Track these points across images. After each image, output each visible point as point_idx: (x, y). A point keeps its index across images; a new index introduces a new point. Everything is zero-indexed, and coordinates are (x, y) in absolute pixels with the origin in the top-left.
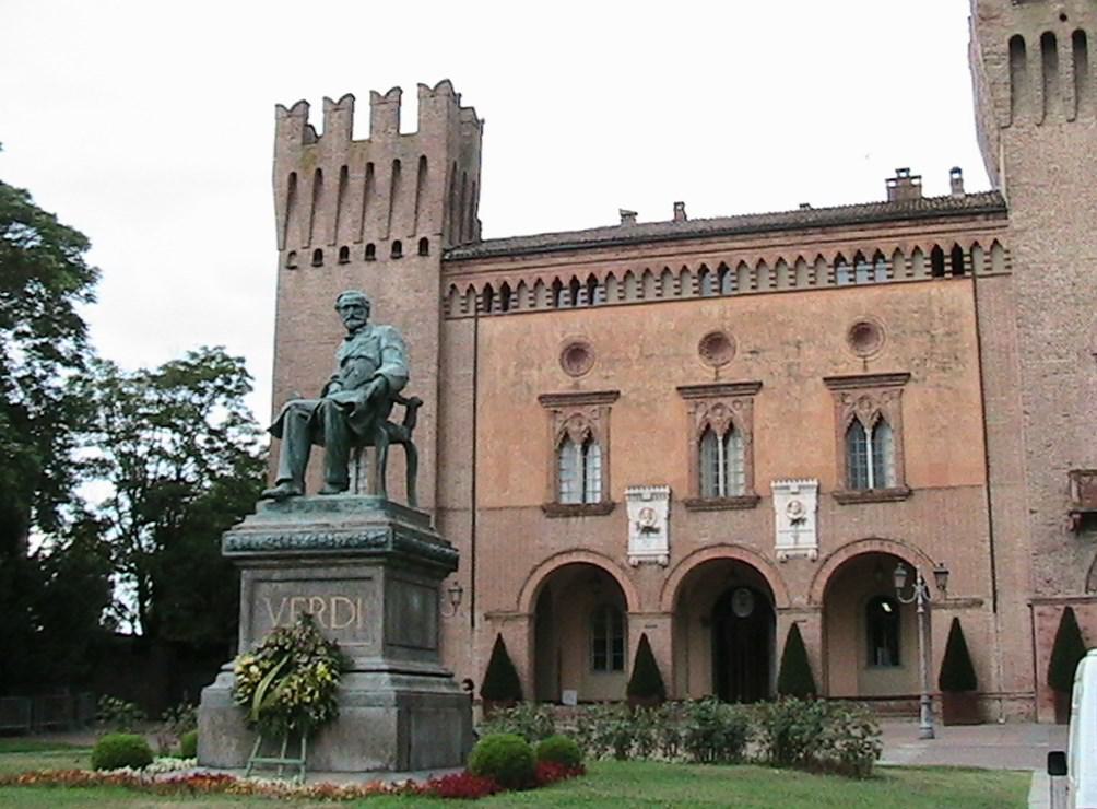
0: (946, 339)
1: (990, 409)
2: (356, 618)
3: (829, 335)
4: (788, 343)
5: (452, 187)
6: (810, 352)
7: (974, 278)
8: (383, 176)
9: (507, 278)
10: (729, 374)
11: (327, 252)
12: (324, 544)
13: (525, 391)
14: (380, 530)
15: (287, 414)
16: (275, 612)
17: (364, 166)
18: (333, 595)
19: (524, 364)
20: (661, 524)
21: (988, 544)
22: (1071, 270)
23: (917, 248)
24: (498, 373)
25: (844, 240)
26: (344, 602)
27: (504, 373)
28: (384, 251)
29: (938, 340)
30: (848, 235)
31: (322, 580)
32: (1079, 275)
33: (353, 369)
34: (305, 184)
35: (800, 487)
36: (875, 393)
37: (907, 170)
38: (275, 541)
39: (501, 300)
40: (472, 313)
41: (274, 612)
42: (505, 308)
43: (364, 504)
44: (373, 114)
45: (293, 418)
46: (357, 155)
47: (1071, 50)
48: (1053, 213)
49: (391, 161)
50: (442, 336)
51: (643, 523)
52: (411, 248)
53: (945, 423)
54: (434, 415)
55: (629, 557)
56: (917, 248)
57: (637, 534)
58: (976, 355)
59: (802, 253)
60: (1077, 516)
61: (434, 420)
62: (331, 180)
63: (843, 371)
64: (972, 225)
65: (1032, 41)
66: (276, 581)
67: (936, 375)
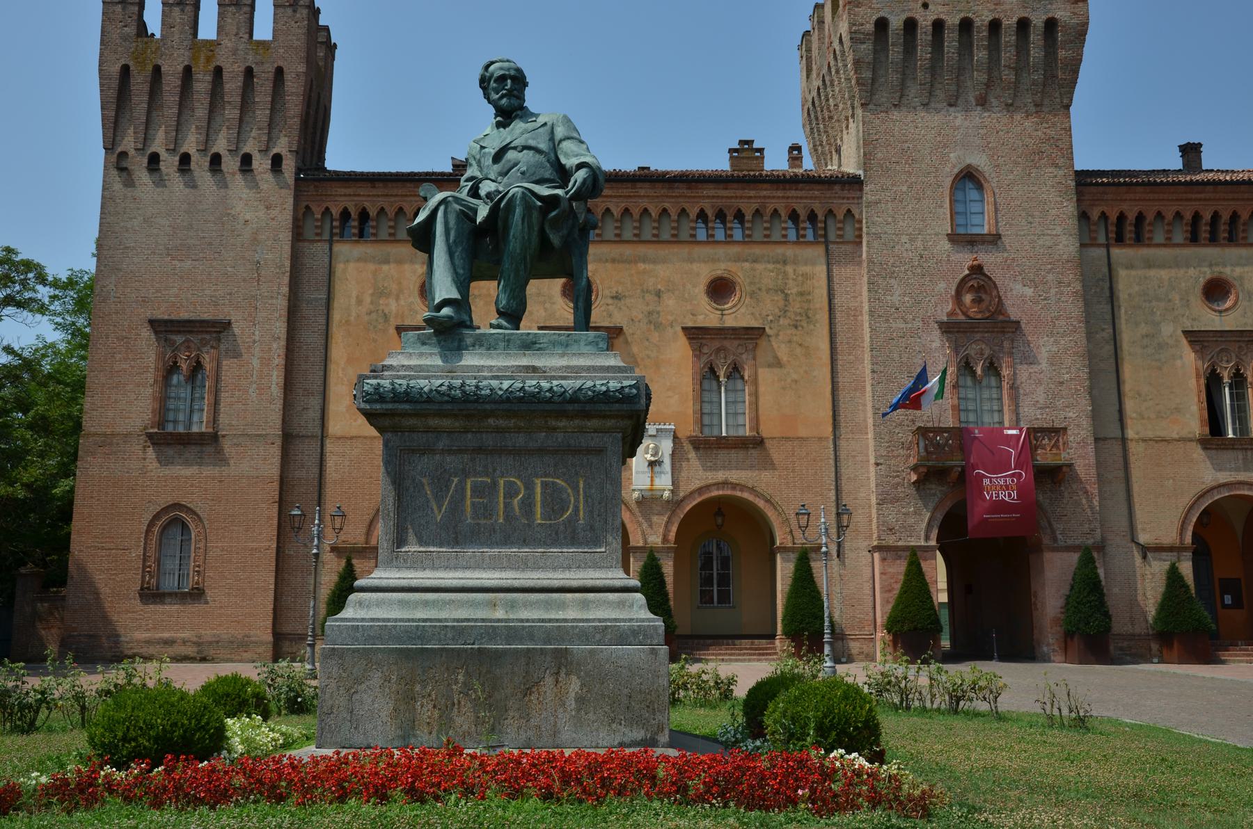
0: (799, 299)
2: (576, 509)
3: (689, 286)
4: (648, 291)
5: (308, 106)
6: (670, 302)
7: (827, 243)
8: (233, 86)
9: (367, 205)
11: (164, 155)
12: (533, 395)
13: (381, 320)
14: (627, 378)
15: (442, 208)
16: (439, 499)
17: (211, 67)
18: (537, 477)
19: (380, 293)
21: (833, 492)
22: (919, 244)
23: (776, 210)
24: (353, 301)
25: (708, 197)
26: (553, 483)
27: (359, 302)
28: (231, 164)
29: (791, 299)
30: (712, 193)
31: (517, 452)
32: (925, 249)
33: (515, 165)
34: (140, 83)
35: (658, 430)
36: (731, 345)
37: (750, 142)
38: (451, 387)
39: (360, 225)
40: (326, 236)
41: (436, 497)
42: (361, 234)
43: (582, 343)
44: (221, 16)
46: (202, 59)
47: (930, 38)
48: (905, 189)
49: (242, 69)
50: (296, 257)
52: (261, 164)
53: (795, 376)
54: (284, 336)
56: (776, 210)
59: (667, 205)
60: (921, 470)
61: (283, 343)
62: (171, 82)
63: (701, 321)
64: (828, 194)
66: (443, 452)
67: (789, 332)
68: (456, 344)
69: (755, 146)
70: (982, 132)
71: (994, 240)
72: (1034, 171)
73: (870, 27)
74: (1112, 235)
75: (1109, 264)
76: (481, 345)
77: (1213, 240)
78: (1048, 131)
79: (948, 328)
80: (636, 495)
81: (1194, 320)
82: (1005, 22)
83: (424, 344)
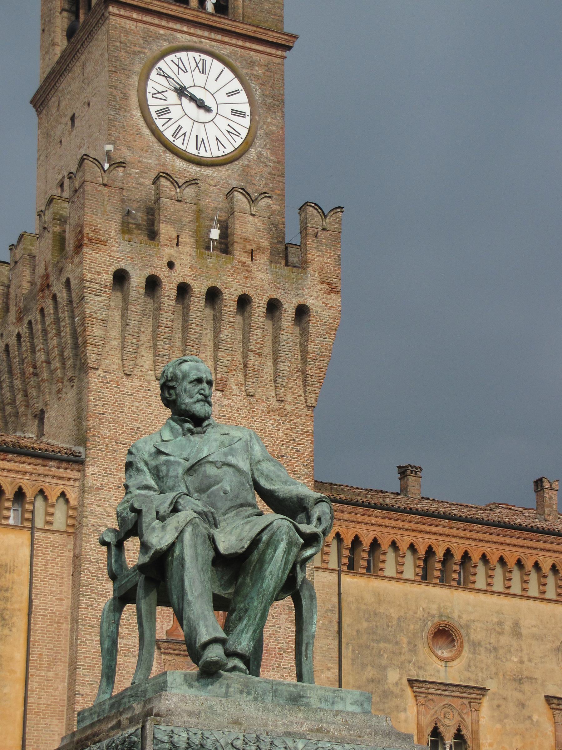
1: (33, 685)
7: (33, 529)
15: (189, 529)
45: (200, 541)
58: (25, 620)
65: (137, 280)
68: (224, 690)
74: (345, 561)
75: (340, 594)
76: (249, 693)
77: (444, 581)
78: (290, 432)
81: (420, 668)
83: (191, 686)
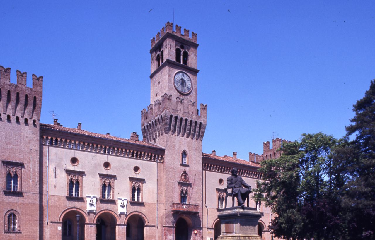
10: (110, 172)
20: (95, 204)
22: (175, 165)
51: (91, 203)
55: (87, 210)
57: (89, 205)
69: (137, 134)
70: (187, 143)
71: (188, 166)
72: (195, 153)
73: (169, 116)
79: (179, 183)
80: (119, 213)
82: (193, 121)
